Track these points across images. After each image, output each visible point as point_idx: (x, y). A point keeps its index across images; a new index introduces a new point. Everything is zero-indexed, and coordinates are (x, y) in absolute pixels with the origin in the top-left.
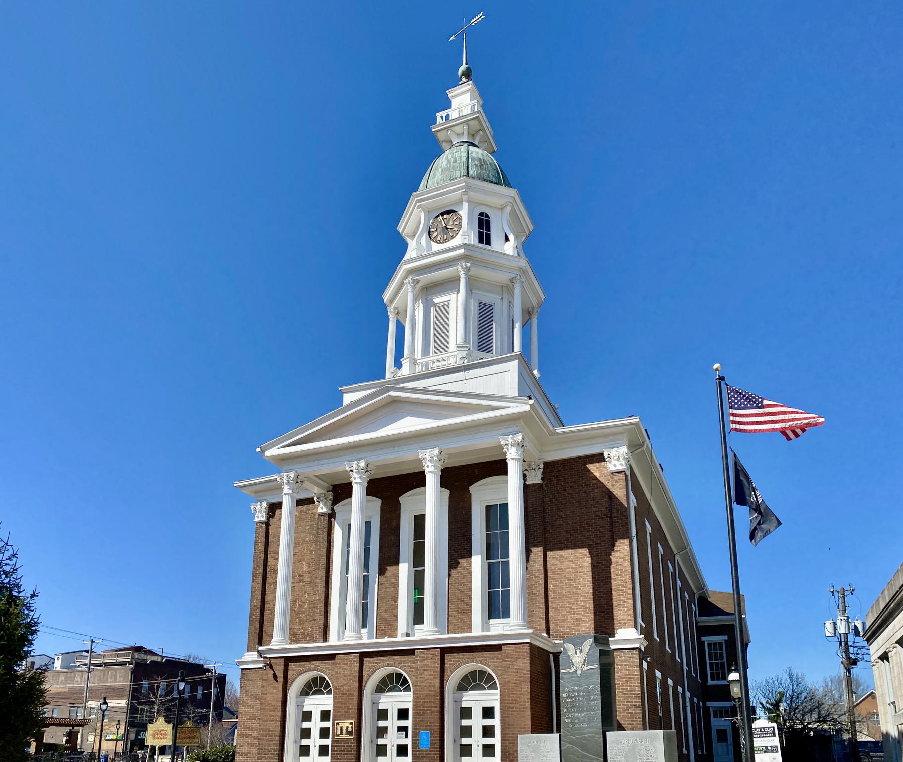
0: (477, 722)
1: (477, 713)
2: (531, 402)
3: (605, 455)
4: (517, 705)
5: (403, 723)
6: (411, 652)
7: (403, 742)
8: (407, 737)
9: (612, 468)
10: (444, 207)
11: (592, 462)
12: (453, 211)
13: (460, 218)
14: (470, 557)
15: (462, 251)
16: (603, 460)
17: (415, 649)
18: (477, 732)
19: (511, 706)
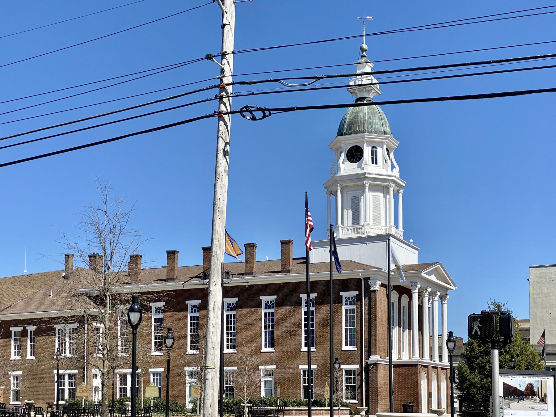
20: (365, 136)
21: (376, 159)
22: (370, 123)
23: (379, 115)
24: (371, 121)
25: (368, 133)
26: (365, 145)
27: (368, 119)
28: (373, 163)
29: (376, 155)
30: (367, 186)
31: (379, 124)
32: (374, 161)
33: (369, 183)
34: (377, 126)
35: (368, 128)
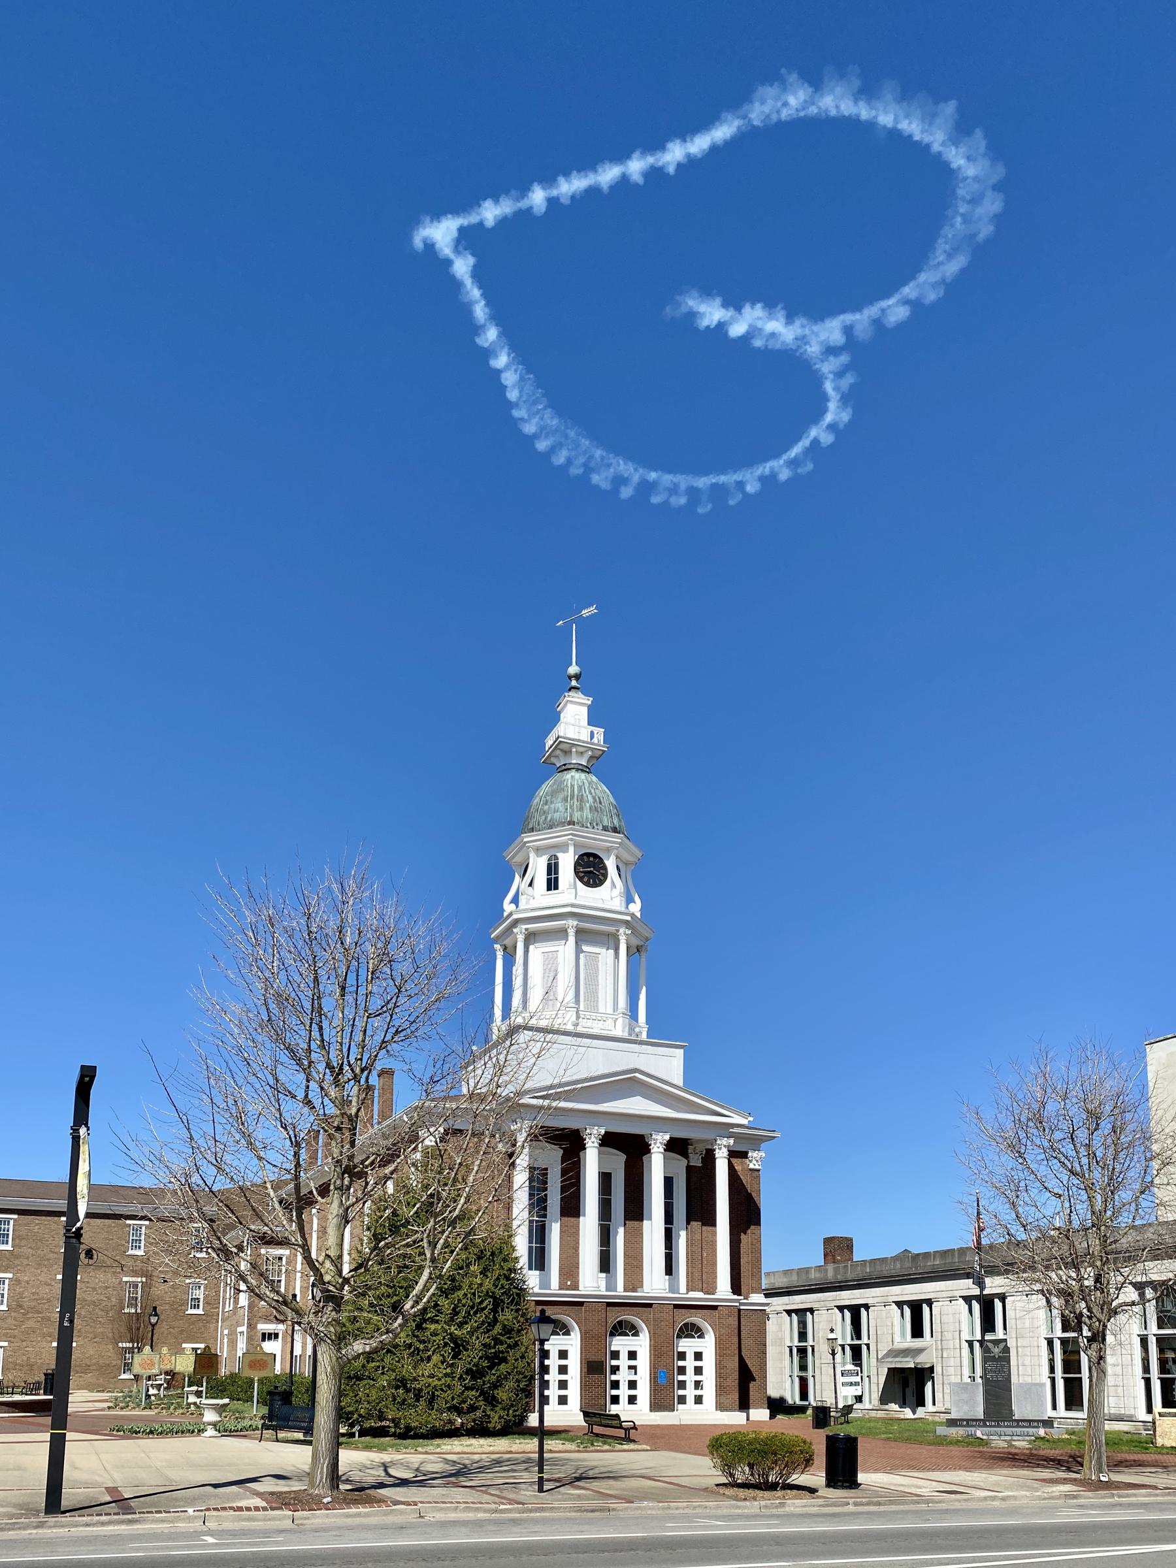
0: (690, 1363)
1: (690, 1356)
2: (751, 1119)
3: (750, 1154)
4: (729, 1352)
5: (632, 1363)
6: (650, 1305)
7: (633, 1378)
8: (636, 1374)
9: (751, 1166)
10: (590, 848)
11: (737, 1157)
12: (600, 858)
13: (605, 868)
14: (642, 1220)
15: (629, 918)
16: (746, 1157)
17: (652, 1304)
18: (690, 1371)
19: (725, 1352)
20: (525, 840)
21: (556, 879)
22: (545, 812)
23: (566, 793)
24: (546, 807)
25: (536, 831)
26: (532, 855)
27: (542, 806)
28: (549, 889)
29: (556, 872)
30: (521, 939)
31: (561, 809)
32: (553, 884)
33: (524, 931)
34: (557, 816)
35: (539, 822)
